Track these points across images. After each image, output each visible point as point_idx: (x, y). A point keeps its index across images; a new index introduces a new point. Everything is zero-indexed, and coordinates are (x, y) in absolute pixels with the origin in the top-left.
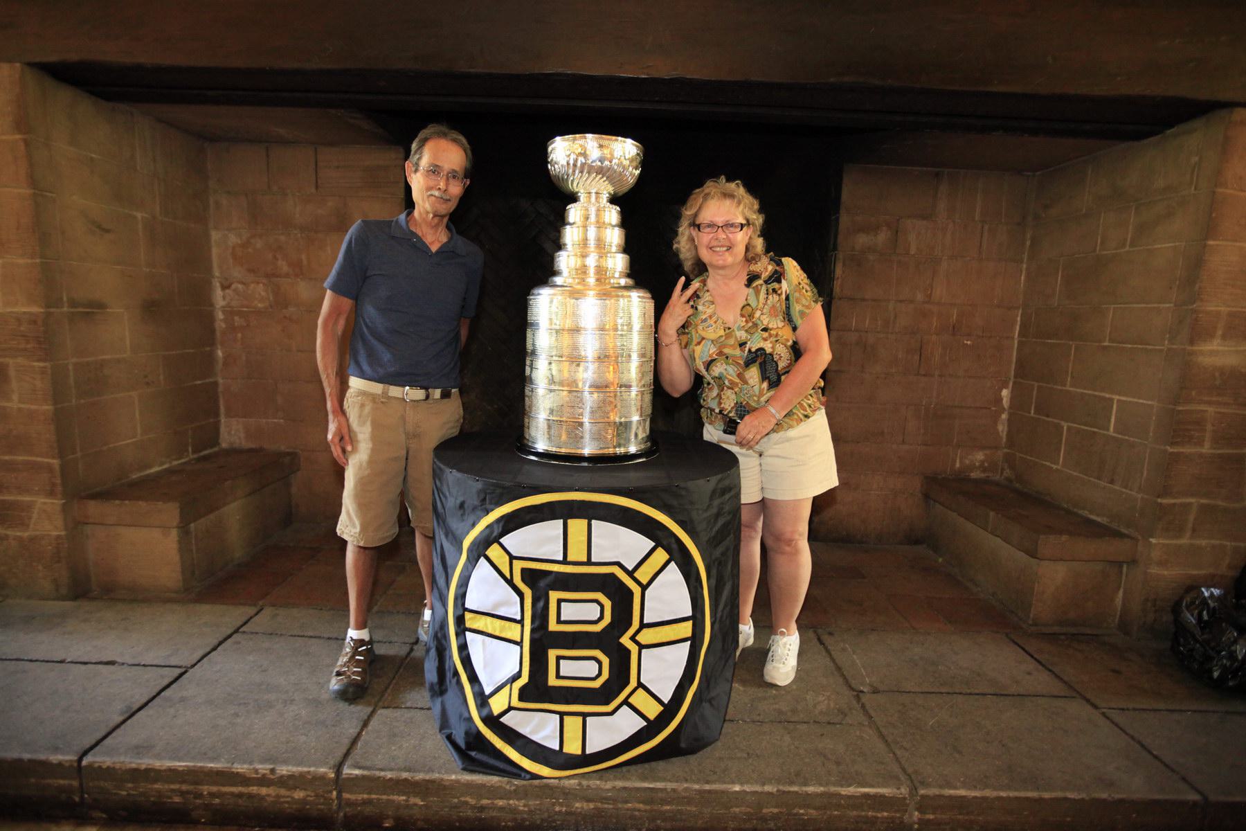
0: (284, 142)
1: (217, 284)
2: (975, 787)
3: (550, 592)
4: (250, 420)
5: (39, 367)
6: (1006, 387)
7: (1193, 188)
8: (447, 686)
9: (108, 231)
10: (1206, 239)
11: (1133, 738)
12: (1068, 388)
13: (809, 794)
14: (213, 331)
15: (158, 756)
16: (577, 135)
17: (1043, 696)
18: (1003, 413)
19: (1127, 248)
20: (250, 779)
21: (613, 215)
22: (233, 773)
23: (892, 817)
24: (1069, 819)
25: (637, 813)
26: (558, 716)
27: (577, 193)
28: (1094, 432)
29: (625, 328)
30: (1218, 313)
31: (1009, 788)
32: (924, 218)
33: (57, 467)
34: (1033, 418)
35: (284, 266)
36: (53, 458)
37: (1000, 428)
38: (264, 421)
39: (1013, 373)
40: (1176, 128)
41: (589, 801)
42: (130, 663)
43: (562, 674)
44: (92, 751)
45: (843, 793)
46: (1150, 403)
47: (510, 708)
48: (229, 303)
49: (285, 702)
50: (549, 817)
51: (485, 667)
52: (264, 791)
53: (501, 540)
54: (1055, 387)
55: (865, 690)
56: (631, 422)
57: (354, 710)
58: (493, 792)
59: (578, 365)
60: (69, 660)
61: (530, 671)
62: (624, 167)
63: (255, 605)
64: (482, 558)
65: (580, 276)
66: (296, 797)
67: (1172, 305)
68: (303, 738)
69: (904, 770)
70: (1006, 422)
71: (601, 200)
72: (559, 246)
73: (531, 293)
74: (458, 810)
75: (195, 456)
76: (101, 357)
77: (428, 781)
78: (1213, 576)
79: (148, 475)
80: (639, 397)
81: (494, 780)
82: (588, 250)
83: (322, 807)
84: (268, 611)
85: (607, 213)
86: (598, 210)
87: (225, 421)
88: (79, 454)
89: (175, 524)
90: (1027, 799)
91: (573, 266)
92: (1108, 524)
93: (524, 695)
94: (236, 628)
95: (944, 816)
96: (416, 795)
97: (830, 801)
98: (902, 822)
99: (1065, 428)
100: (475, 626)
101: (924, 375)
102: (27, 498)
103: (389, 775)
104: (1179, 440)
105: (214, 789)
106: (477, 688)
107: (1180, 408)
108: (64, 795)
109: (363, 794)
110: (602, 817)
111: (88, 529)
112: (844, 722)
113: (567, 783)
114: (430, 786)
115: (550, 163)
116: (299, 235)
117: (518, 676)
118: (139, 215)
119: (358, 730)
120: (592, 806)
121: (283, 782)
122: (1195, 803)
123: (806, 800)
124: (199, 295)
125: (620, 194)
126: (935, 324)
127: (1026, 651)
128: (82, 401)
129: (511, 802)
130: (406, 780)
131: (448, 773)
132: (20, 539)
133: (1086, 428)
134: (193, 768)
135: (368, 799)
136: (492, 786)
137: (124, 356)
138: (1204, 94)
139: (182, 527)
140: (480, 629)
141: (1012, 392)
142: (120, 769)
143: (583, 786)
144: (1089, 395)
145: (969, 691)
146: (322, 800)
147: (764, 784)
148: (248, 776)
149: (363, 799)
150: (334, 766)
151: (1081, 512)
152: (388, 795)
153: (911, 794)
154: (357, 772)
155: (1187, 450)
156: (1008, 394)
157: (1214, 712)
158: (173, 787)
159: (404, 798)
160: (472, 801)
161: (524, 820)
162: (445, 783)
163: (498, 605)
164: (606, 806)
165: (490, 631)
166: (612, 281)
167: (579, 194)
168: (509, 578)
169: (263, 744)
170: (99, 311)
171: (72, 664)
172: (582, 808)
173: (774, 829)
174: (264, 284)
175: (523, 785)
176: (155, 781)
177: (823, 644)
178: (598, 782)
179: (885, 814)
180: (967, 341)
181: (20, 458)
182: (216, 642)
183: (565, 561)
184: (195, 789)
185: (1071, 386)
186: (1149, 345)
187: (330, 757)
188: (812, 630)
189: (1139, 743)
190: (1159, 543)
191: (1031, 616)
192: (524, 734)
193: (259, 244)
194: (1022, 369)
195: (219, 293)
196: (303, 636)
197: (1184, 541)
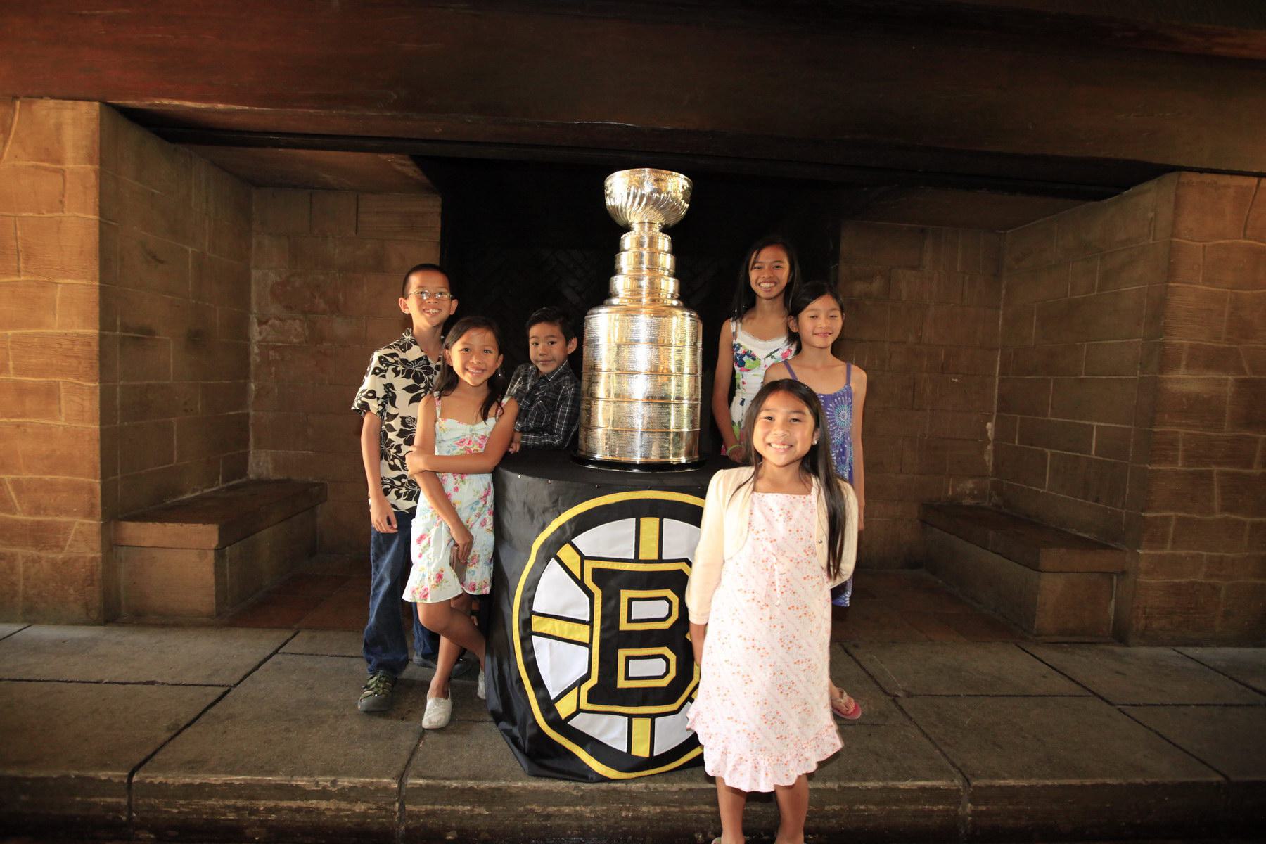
0: (328, 188)
1: (254, 319)
2: (1022, 777)
3: (621, 591)
4: (280, 451)
5: (89, 386)
6: (990, 421)
7: (1152, 238)
8: (509, 694)
9: (161, 262)
10: (1168, 282)
11: (1150, 729)
12: (1049, 418)
13: (868, 789)
14: (248, 365)
15: (213, 771)
16: (634, 170)
17: (1062, 696)
18: (988, 444)
19: (1096, 293)
20: (308, 791)
21: (664, 243)
22: (292, 785)
23: (948, 810)
24: (1108, 805)
25: (703, 816)
26: (627, 718)
27: (631, 223)
28: (1078, 456)
29: (678, 343)
30: (1182, 345)
31: (1054, 777)
32: (913, 268)
33: (99, 487)
34: (1017, 447)
35: (321, 304)
36: (95, 478)
37: (987, 458)
38: (293, 452)
39: (995, 406)
40: (1131, 190)
41: (655, 804)
42: (170, 681)
43: (630, 675)
44: (142, 767)
45: (901, 787)
46: (1127, 426)
47: (579, 711)
48: (264, 339)
49: (336, 716)
50: (616, 823)
51: (552, 670)
52: (323, 804)
53: (573, 541)
54: (1037, 418)
55: (900, 695)
56: (682, 432)
57: (407, 723)
58: (560, 799)
59: (637, 377)
60: (104, 682)
61: (599, 672)
62: (678, 199)
63: (289, 628)
64: (553, 560)
65: (639, 297)
66: (357, 811)
67: (1141, 340)
68: (361, 751)
69: (953, 765)
70: (992, 454)
71: (654, 230)
72: (612, 270)
73: (589, 313)
74: (525, 819)
75: (225, 486)
76: (147, 382)
77: (490, 788)
78: (1193, 584)
79: (179, 502)
80: (691, 410)
81: (561, 785)
82: (644, 273)
83: (384, 820)
84: (304, 635)
85: (660, 241)
86: (652, 241)
87: (254, 453)
88: (119, 476)
89: (214, 546)
90: (1070, 786)
91: (629, 287)
92: (1095, 539)
93: (593, 696)
94: (274, 649)
95: (995, 807)
96: (481, 804)
97: (889, 795)
98: (956, 815)
99: (1049, 454)
100: (542, 630)
101: (918, 410)
102: (64, 519)
103: (454, 784)
104: (1157, 459)
105: (271, 804)
106: (541, 694)
107: (1155, 430)
108: (111, 814)
109: (427, 804)
110: (668, 820)
111: (122, 552)
112: (886, 724)
113: (633, 786)
114: (496, 795)
115: (609, 195)
116: (338, 275)
117: (587, 677)
118: (190, 250)
119: (415, 742)
120: (658, 809)
121: (344, 794)
122: (1218, 782)
123: (866, 797)
124: (239, 328)
125: (671, 225)
126: (926, 363)
127: (1036, 657)
128: (126, 423)
129: (578, 808)
130: (471, 788)
131: (515, 779)
132: (54, 563)
133: (1068, 453)
134: (249, 782)
135: (431, 810)
136: (559, 792)
137: (168, 382)
138: (1157, 160)
139: (218, 549)
140: (547, 632)
141: (996, 425)
142: (173, 784)
143: (650, 789)
144: (1070, 423)
145: (995, 693)
146: (384, 813)
147: (825, 781)
148: (307, 789)
149: (426, 810)
150: (398, 776)
151: (1069, 530)
152: (453, 806)
153: (963, 786)
154: (421, 782)
155: (1164, 467)
156: (992, 429)
157: (1215, 705)
158: (227, 802)
159: (469, 808)
160: (538, 809)
161: (590, 827)
162: (512, 791)
163: (566, 608)
164: (672, 809)
165: (558, 634)
166: (665, 302)
167: (633, 224)
168: (579, 578)
169: (321, 757)
170: (145, 336)
171: (111, 685)
172: (649, 812)
173: (836, 826)
174: (300, 320)
175: (591, 790)
176: (210, 797)
177: (851, 655)
178: (665, 785)
179: (941, 807)
180: (954, 378)
181: (61, 478)
182: (256, 663)
183: (637, 560)
184: (253, 804)
185: (1052, 416)
186: (1123, 375)
187: (392, 768)
188: (837, 643)
189: (1156, 733)
190: (1146, 554)
191: (1035, 627)
192: (591, 735)
193: (298, 282)
194: (1005, 404)
195: (255, 328)
196: (345, 656)
197: (1168, 551)
